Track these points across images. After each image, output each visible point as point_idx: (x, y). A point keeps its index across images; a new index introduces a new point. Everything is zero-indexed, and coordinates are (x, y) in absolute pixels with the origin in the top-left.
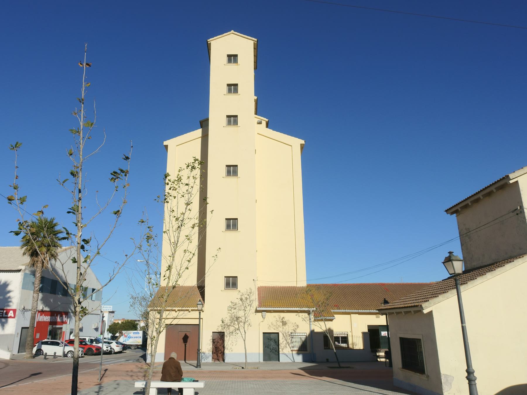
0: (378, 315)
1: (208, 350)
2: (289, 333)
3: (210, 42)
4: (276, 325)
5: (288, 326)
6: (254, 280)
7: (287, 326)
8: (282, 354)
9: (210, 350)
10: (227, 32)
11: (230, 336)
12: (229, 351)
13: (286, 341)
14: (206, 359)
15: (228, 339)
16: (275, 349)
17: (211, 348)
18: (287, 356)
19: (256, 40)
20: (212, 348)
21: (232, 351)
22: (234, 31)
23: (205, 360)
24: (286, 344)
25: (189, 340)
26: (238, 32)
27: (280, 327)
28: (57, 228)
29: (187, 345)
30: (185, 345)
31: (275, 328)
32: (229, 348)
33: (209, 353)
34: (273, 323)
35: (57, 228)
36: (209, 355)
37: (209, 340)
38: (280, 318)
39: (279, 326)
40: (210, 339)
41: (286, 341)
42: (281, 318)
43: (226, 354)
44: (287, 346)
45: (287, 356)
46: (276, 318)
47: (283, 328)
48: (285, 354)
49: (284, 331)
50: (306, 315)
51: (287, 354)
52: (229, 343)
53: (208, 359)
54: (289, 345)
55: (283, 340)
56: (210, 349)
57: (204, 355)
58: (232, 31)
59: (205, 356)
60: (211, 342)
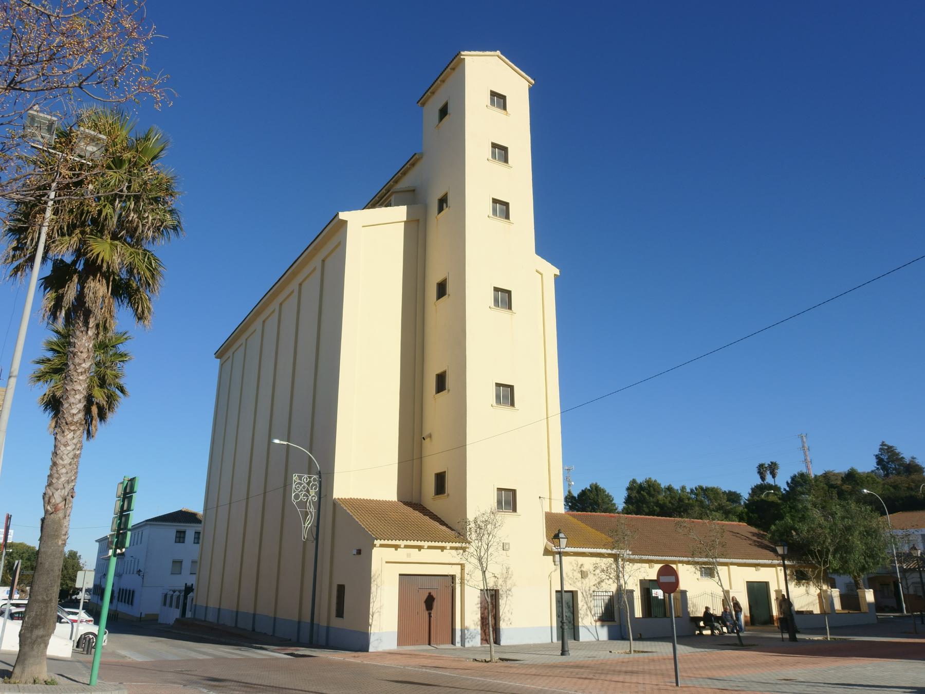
0: (652, 563)
1: (474, 624)
2: (591, 592)
3: (464, 57)
4: (573, 577)
5: (589, 579)
6: (540, 497)
7: (587, 579)
8: (583, 626)
9: (477, 623)
10: (491, 51)
11: (507, 597)
12: (507, 625)
13: (587, 605)
14: (472, 641)
15: (504, 603)
16: (569, 619)
17: (478, 619)
18: (589, 630)
19: (533, 82)
20: (480, 618)
21: (511, 623)
22: (501, 54)
23: (470, 641)
24: (587, 610)
25: (435, 604)
26: (475, 51)
27: (579, 581)
28: (54, 338)
29: (432, 615)
30: (430, 614)
31: (572, 583)
32: (506, 619)
33: (475, 629)
34: (568, 574)
35: (54, 338)
36: (475, 632)
37: (476, 605)
38: (577, 565)
39: (576, 579)
40: (476, 603)
41: (587, 605)
42: (579, 566)
43: (502, 629)
44: (589, 613)
45: (589, 630)
46: (573, 566)
47: (582, 583)
48: (586, 627)
49: (583, 588)
50: (611, 560)
51: (589, 627)
52: (506, 610)
53: (474, 640)
54: (591, 612)
55: (583, 603)
56: (477, 620)
57: (468, 633)
58: (498, 53)
59: (470, 635)
60: (478, 608)
